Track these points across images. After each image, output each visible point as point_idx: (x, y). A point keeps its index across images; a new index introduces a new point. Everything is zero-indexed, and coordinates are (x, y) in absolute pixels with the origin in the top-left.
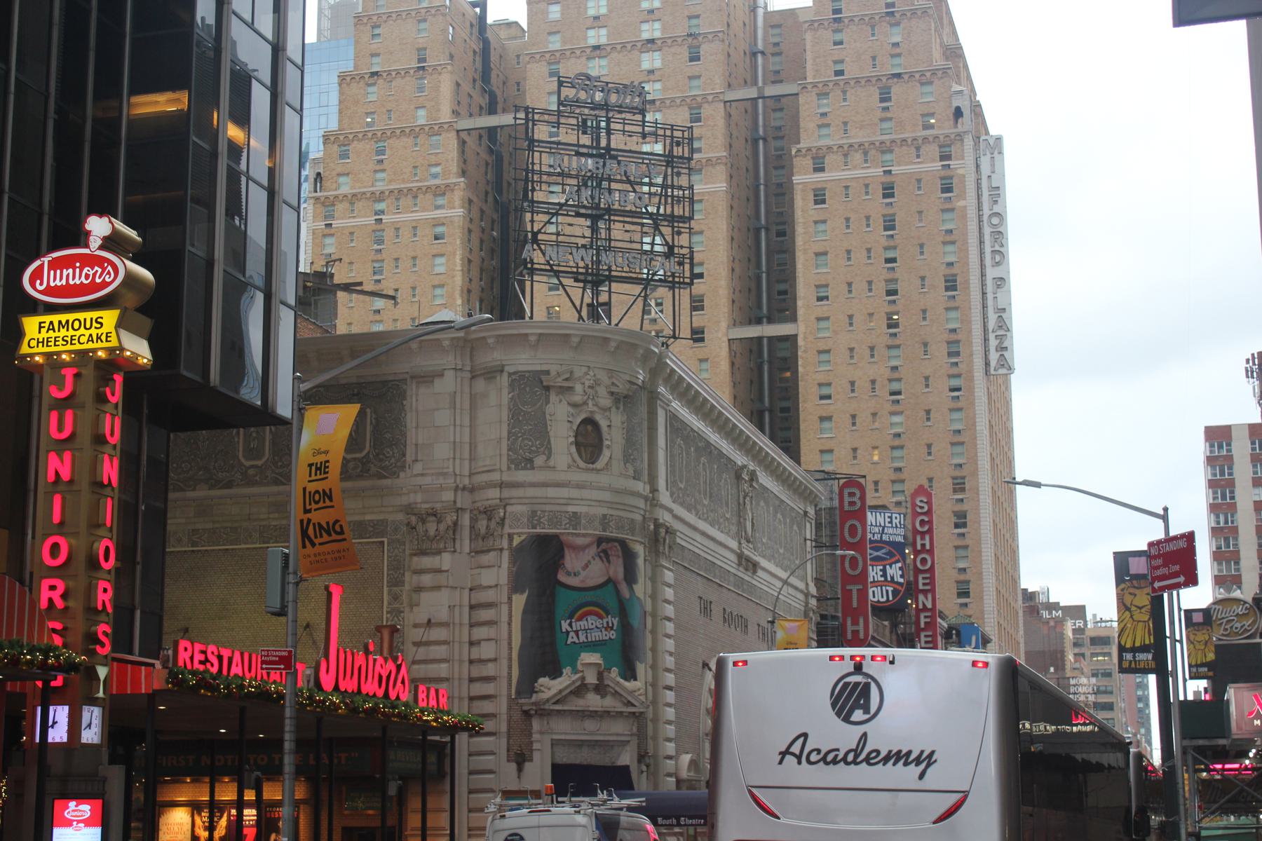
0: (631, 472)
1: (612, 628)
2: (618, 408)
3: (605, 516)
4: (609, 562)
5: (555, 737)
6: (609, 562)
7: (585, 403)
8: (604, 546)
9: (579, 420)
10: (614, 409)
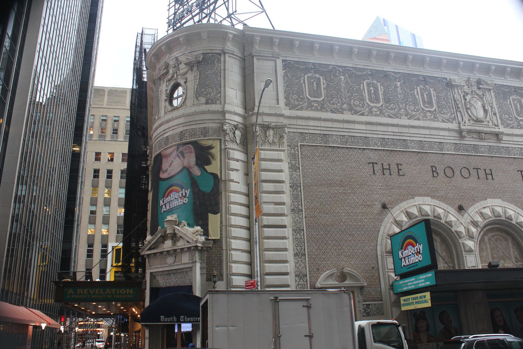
0: (203, 100)
1: (185, 197)
2: (192, 70)
3: (182, 132)
5: (152, 271)
6: (184, 157)
7: (173, 77)
8: (181, 149)
9: (170, 87)
10: (190, 71)
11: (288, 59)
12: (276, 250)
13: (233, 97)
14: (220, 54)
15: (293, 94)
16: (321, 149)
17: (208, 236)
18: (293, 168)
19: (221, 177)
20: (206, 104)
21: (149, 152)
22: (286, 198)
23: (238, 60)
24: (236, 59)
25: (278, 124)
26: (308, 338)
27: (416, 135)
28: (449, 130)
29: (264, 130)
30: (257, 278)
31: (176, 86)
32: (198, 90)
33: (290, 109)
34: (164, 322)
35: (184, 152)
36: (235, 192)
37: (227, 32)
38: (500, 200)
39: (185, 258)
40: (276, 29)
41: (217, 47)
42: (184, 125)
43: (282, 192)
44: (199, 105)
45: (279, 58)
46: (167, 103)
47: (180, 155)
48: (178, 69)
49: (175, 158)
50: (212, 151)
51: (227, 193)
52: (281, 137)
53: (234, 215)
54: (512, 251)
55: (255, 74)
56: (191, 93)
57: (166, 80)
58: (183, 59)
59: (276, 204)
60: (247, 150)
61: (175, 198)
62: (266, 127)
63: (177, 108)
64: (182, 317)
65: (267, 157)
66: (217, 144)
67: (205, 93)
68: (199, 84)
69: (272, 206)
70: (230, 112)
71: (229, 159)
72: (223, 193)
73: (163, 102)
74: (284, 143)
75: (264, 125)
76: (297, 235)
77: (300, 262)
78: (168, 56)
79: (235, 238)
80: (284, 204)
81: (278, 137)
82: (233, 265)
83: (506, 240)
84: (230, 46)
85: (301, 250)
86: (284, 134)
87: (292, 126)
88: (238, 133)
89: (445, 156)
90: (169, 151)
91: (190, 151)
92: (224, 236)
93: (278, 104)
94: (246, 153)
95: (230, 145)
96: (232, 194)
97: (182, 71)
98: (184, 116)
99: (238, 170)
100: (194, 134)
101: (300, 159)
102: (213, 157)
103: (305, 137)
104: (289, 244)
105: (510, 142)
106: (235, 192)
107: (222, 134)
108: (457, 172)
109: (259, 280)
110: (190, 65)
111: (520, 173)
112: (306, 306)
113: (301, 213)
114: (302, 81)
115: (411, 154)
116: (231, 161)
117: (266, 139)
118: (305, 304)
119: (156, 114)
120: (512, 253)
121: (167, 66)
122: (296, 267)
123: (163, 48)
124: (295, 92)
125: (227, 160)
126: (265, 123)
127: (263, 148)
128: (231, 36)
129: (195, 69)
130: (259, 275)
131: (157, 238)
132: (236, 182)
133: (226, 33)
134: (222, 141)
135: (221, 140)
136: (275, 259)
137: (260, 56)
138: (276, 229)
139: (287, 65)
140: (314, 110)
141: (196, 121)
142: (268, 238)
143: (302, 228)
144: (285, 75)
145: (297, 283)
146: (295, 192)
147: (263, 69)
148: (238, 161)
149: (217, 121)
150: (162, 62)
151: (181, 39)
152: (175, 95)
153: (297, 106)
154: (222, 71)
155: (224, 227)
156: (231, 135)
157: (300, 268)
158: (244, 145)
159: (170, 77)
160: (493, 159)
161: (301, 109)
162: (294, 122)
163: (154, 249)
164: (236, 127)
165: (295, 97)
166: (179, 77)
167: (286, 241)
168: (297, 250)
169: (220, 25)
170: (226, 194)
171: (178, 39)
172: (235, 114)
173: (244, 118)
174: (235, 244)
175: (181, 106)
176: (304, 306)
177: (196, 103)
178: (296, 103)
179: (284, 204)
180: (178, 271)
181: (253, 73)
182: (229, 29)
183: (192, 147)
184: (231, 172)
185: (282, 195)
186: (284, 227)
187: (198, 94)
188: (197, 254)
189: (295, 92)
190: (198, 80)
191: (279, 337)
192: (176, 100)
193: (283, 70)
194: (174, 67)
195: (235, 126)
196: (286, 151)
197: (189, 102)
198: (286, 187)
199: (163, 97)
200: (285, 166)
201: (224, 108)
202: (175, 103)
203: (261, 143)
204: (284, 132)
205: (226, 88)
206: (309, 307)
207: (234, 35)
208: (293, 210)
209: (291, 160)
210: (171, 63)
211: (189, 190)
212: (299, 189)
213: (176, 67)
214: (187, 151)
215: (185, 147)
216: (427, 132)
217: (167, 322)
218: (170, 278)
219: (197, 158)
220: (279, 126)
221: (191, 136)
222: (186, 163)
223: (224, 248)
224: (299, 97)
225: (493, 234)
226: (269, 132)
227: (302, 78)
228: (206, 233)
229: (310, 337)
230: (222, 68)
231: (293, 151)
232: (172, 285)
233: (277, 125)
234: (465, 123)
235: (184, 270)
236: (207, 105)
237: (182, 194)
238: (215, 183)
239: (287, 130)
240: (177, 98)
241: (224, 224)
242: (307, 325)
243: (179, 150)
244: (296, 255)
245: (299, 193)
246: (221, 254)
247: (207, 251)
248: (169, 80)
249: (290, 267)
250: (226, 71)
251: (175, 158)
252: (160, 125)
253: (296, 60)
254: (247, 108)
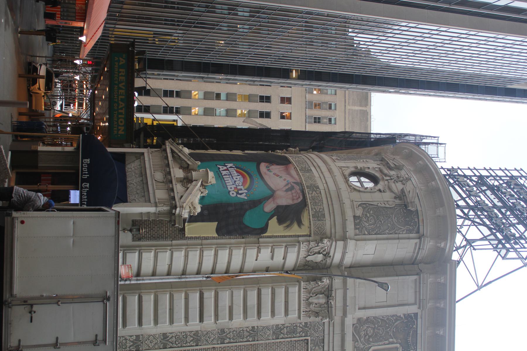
1: (238, 193)
2: (395, 198)
3: (318, 187)
4: (287, 191)
5: (146, 155)
6: (287, 191)
7: (386, 175)
8: (297, 188)
9: (373, 172)
10: (394, 195)
11: (419, 320)
12: (171, 310)
13: (365, 251)
14: (418, 232)
15: (374, 329)
17: (189, 222)
18: (278, 331)
19: (264, 237)
20: (355, 217)
21: (292, 151)
22: (238, 321)
23: (413, 256)
24: (414, 252)
25: (333, 309)
26: (53, 341)
29: (325, 291)
30: (134, 280)
31: (374, 179)
32: (371, 207)
33: (353, 325)
34: (82, 163)
35: (293, 191)
36: (244, 254)
37: (447, 239)
39: (161, 194)
40: (457, 304)
41: (427, 228)
42: (327, 190)
43: (245, 316)
44: (352, 207)
45: (419, 308)
46: (353, 169)
47: (290, 186)
48: (395, 182)
49: (285, 180)
50: (295, 226)
51: (242, 245)
52: (317, 314)
53: (216, 255)
55: (396, 278)
56: (366, 197)
57: (381, 167)
58: (409, 187)
59: (231, 309)
60: (298, 270)
61: (235, 181)
62: (328, 293)
63: (347, 181)
64: (88, 185)
65: (290, 295)
66: (304, 231)
67: (368, 215)
68: (377, 207)
69: (227, 304)
70: (345, 247)
71: (286, 246)
72: (243, 240)
73: (354, 165)
74: (310, 317)
75: (332, 290)
76: (191, 336)
77: (155, 341)
78: (412, 169)
79: (186, 256)
80: (231, 318)
81: (317, 309)
82: (152, 254)
84: (429, 244)
85: (172, 343)
86: (320, 318)
87: (331, 328)
88: (319, 258)
90: (293, 172)
91: (295, 198)
92: (190, 242)
93: (359, 309)
94: (295, 269)
95: (304, 248)
96: (242, 251)
97: (393, 186)
98: (338, 189)
99: (272, 258)
100: (316, 202)
101: (289, 340)
102: (288, 227)
103: (319, 346)
104: (179, 326)
106: (244, 254)
107: (318, 238)
109: (133, 282)
110: (401, 196)
112: (96, 339)
113: (219, 342)
114: (391, 340)
116: (283, 249)
117: (313, 294)
118: (100, 337)
119: (339, 157)
121: (398, 168)
122: (150, 336)
123: (420, 162)
124: (376, 330)
125: (284, 244)
126: (333, 292)
127: (302, 290)
128: (442, 245)
129: (398, 201)
130: (139, 282)
131: (186, 160)
133: (446, 239)
134: (308, 238)
135: (310, 236)
136: (159, 308)
137: (420, 283)
138: (198, 309)
139: (411, 319)
141: (332, 204)
142: (187, 299)
143: (200, 344)
144: (397, 318)
145: (128, 338)
146: (246, 334)
147: (403, 287)
148: (285, 258)
149: (333, 231)
150: (403, 162)
151: (433, 183)
152: (363, 179)
153: (358, 333)
154: (396, 236)
155: (199, 241)
156: (317, 249)
157: (148, 342)
158: (304, 265)
159: (386, 171)
161: (355, 340)
162: (338, 330)
163: (173, 156)
164: (327, 255)
165: (370, 331)
166: (386, 182)
167: (183, 322)
168: (172, 338)
169: (455, 230)
170: (241, 243)
171: (434, 179)
172: (344, 254)
173: (340, 265)
174: (179, 256)
175: (349, 186)
176: (96, 336)
177: (355, 203)
178: (362, 333)
179: (231, 318)
180: (145, 186)
181: (397, 276)
182: (451, 242)
183: (300, 200)
184: (270, 250)
185: (242, 316)
186: (201, 320)
187: (364, 205)
188: (166, 208)
189: (376, 330)
190: (383, 205)
191: (57, 303)
192: (357, 180)
193: (404, 315)
194: (398, 177)
196: (299, 321)
197: (355, 196)
198: (253, 321)
199: (360, 165)
200: (280, 319)
201: (351, 239)
202: (353, 179)
203: (308, 287)
204: (323, 317)
205: (376, 242)
206: (95, 343)
207: (444, 250)
208: (223, 331)
209: (287, 327)
210: (403, 173)
211: (246, 198)
212: (251, 339)
213: (398, 179)
214: (294, 194)
215: (299, 191)
217: (82, 167)
218: (137, 176)
219: (287, 207)
220: (331, 311)
221: (313, 198)
222: (279, 193)
223: (174, 242)
224: (369, 337)
226: (323, 298)
227: (395, 340)
228: (193, 219)
229: (56, 345)
230: (400, 236)
231: (299, 329)
232: (128, 179)
233: (331, 307)
235: (146, 193)
236: (352, 218)
237: (241, 190)
238: (255, 229)
239: (326, 321)
240: (359, 181)
241: (205, 242)
242: (71, 339)
243: (295, 185)
244: (165, 335)
245: (245, 340)
246: (166, 239)
247: (170, 221)
248: (381, 171)
249: (149, 328)
250: (397, 241)
251: (285, 180)
252: (324, 162)
253: (419, 332)
254: (351, 269)
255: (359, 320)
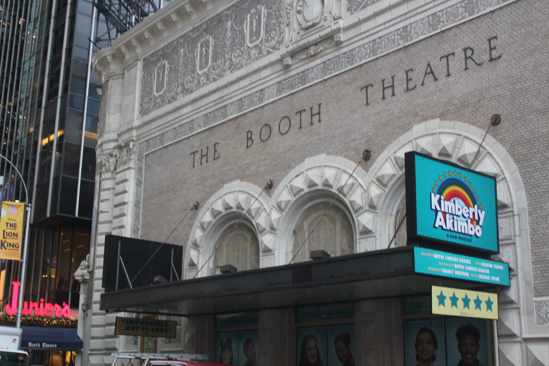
16: (158, 153)
18: (138, 184)
27: (236, 93)
28: (271, 64)
38: (324, 155)
45: (140, 60)
54: (338, 238)
70: (106, 142)
83: (333, 221)
89: (265, 108)
99: (108, 200)
105: (356, 39)
108: (275, 129)
111: (365, 90)
115: (229, 123)
120: (338, 242)
132: (105, 212)
137: (128, 66)
140: (158, 108)
144: (144, 77)
148: (109, 189)
160: (327, 83)
162: (146, 128)
195: (109, 154)
216: (246, 82)
225: (316, 215)
234: (291, 41)
253: (152, 52)
255: (140, 113)
